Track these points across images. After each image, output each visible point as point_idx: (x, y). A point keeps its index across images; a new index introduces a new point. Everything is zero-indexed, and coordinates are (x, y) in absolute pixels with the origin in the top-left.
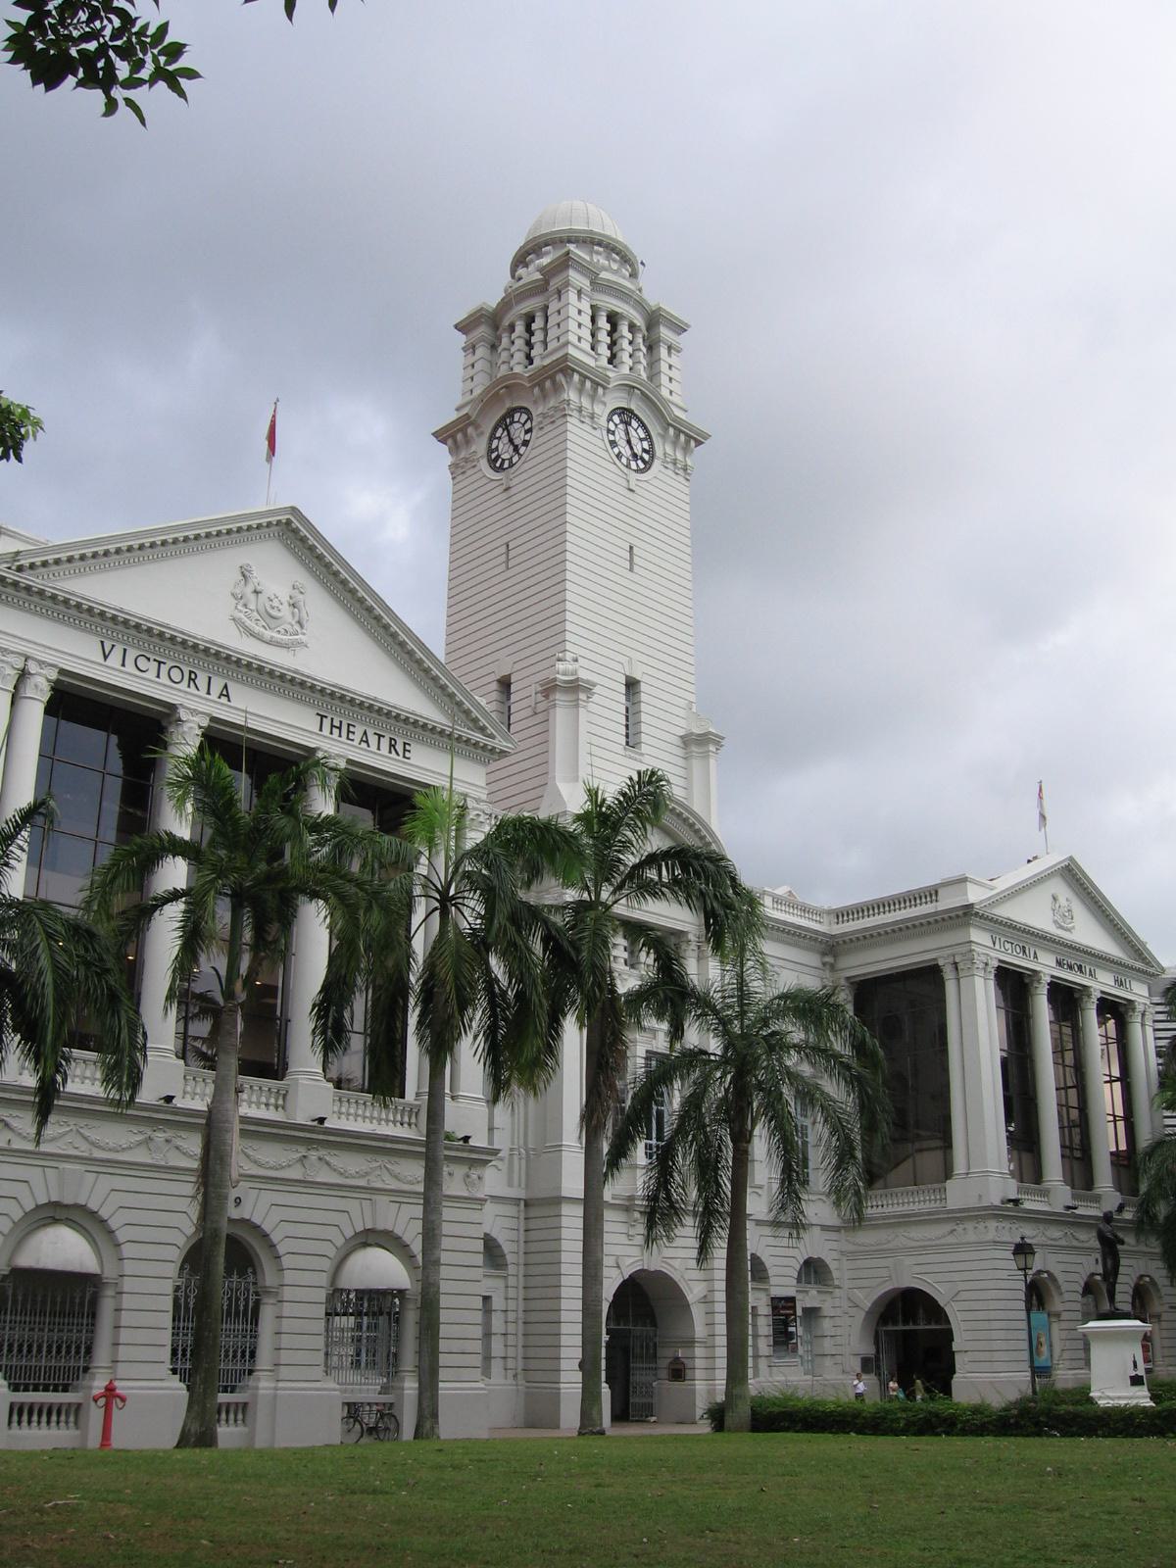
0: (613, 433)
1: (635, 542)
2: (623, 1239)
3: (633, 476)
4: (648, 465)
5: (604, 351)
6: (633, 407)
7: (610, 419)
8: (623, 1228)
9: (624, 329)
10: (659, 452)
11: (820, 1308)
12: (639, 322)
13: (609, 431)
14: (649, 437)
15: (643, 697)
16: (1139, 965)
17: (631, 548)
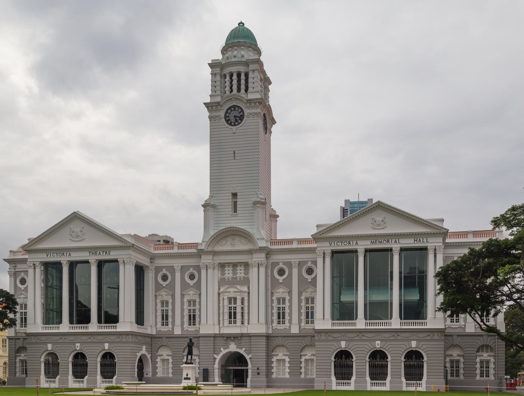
0: (228, 117)
1: (234, 149)
2: (224, 344)
3: (234, 128)
4: (242, 120)
5: (228, 88)
6: (234, 104)
7: (227, 112)
8: (223, 341)
9: (235, 77)
10: (246, 114)
12: (242, 69)
13: (227, 117)
14: (242, 111)
15: (238, 197)
16: (435, 231)
17: (234, 152)
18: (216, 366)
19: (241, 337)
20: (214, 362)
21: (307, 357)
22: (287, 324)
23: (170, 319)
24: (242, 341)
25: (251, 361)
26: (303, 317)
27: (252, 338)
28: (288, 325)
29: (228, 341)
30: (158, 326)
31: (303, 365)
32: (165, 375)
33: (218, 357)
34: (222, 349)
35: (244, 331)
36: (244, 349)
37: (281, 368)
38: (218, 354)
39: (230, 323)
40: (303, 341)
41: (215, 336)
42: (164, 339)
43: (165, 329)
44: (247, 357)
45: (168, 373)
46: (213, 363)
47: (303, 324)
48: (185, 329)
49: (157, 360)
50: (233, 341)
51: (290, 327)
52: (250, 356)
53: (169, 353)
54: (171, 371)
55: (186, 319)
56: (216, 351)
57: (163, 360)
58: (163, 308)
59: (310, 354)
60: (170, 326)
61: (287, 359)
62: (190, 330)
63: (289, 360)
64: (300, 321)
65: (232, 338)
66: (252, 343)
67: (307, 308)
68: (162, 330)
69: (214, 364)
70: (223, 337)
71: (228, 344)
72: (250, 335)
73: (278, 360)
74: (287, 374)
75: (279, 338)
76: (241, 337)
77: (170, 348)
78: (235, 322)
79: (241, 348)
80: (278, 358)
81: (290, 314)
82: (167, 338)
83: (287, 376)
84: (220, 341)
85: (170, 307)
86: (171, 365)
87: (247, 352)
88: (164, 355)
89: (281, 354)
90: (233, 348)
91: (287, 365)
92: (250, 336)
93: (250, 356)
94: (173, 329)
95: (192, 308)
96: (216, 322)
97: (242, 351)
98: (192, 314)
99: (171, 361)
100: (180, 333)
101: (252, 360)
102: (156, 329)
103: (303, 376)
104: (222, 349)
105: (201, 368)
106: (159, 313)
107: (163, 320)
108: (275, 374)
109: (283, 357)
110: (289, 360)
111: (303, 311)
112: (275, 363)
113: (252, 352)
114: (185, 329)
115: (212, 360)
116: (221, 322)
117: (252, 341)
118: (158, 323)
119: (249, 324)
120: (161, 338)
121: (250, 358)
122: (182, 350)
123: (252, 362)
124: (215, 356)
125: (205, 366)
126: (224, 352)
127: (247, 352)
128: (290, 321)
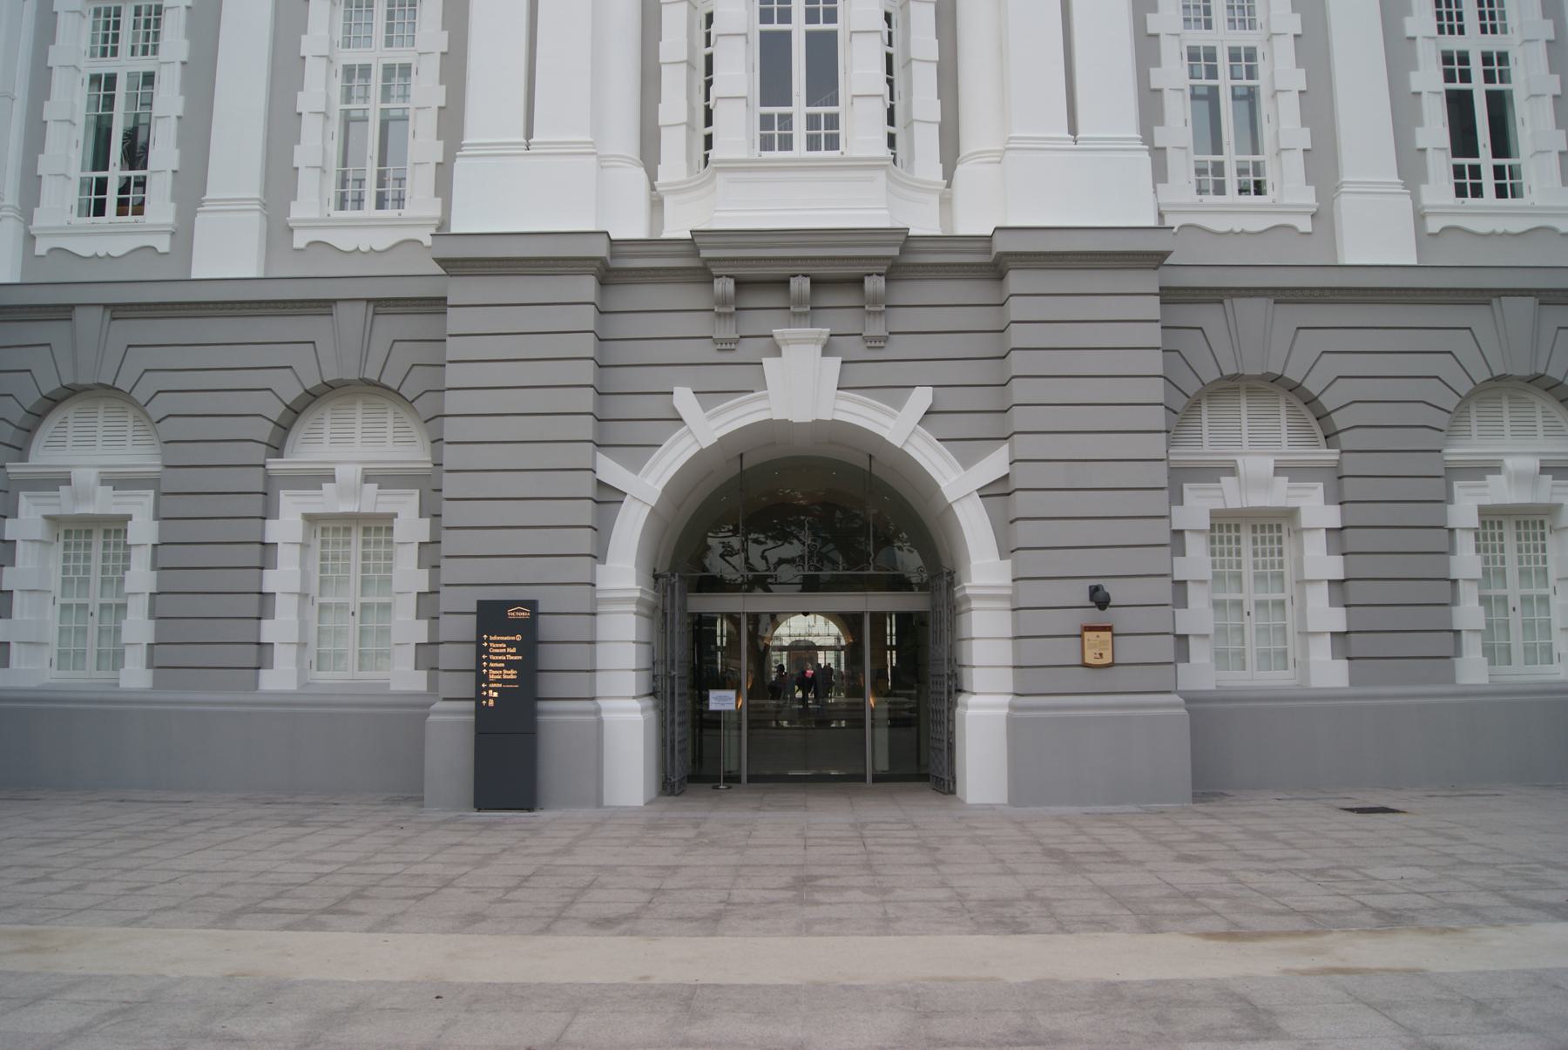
2: (707, 352)
8: (700, 324)
11: (1560, 505)
18: (623, 573)
19: (896, 271)
20: (601, 531)
21: (1499, 491)
22: (1291, 189)
23: (163, 154)
24: (902, 320)
25: (1004, 527)
26: (1435, 131)
27: (1016, 280)
28: (1307, 197)
29: (754, 322)
30: (42, 219)
31: (1466, 562)
32: (86, 678)
33: (646, 485)
34: (684, 400)
35: (923, 222)
36: (922, 398)
37: (1250, 594)
38: (638, 451)
39: (774, 134)
40: (1460, 343)
41: (613, 269)
42: (89, 322)
43: (111, 239)
44: (957, 482)
45: (117, 658)
46: (583, 541)
47: (1439, 187)
48: (300, 240)
49: (11, 529)
50: (810, 312)
51: (1323, 216)
52: (995, 464)
53: (140, 456)
54: (138, 628)
55: (315, 147)
56: (619, 423)
57: (74, 531)
58: (105, 67)
59: (1533, 464)
60: (160, 206)
61: (1317, 510)
62: (345, 240)
63: (1332, 516)
64: (1410, 167)
65: (800, 286)
66: (1018, 336)
67: (1456, 66)
68: (84, 247)
69: (599, 556)
70: (703, 275)
71: (746, 351)
72: (1002, 245)
73: (1225, 524)
74: (1321, 651)
75: (1240, 304)
76: (896, 271)
77: (142, 408)
78: (825, 134)
79: (893, 392)
80: (1230, 495)
81: (1318, 105)
82: (119, 311)
83: (1328, 672)
84: (671, 319)
85: (174, 42)
86: (141, 577)
87: (963, 426)
88: (85, 476)
89: (1255, 464)
90: (802, 385)
91: (1322, 563)
92: (992, 264)
93: (995, 464)
94: (183, 235)
95: (376, 55)
96: (623, 137)
97: (898, 425)
98: (374, 108)
99: (143, 530)
100: (250, 268)
101: (1022, 503)
102: (30, 239)
103: (1473, 669)
104: (684, 400)
105: (448, 599)
106: (70, 105)
107: (100, 160)
108: (1200, 653)
109: (1280, 494)
110: (1332, 516)
111: (1429, 81)
112: (1197, 547)
113: (1019, 419)
114: (300, 240)
115: (585, 512)
116: (675, 148)
117: (1017, 308)
118: (49, 189)
119: (950, 152)
120: (64, 312)
121: (996, 492)
122: (265, 431)
123: (1025, 533)
124: (611, 470)
125: (504, 578)
126: (703, 427)
127: (963, 426)
128: (1322, 163)
